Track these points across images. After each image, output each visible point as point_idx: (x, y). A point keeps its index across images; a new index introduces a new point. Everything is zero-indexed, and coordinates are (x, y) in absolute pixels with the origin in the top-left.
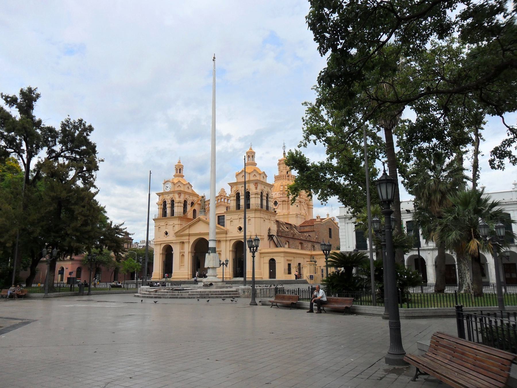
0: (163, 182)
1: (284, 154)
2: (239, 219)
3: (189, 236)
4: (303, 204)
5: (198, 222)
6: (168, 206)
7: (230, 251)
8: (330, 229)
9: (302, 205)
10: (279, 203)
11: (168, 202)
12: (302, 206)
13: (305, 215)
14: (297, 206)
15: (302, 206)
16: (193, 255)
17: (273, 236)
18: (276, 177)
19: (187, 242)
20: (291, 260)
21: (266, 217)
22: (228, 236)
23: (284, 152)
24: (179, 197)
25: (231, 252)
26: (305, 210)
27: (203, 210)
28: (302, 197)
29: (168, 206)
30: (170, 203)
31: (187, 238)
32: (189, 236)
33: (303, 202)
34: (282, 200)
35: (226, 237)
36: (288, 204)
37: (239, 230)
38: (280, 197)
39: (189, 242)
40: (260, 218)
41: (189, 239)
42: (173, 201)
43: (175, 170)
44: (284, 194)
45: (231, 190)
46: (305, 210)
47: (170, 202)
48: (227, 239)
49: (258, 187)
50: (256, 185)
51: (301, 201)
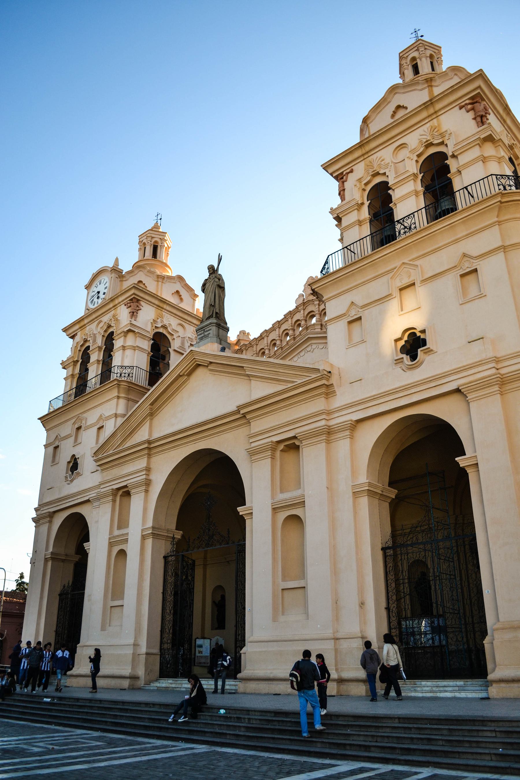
0: (86, 281)
2: (396, 293)
3: (149, 456)
6: (95, 356)
7: (356, 494)
16: (165, 548)
19: (137, 485)
22: (338, 401)
24: (133, 314)
25: (364, 501)
27: (213, 320)
29: (95, 356)
30: (100, 348)
31: (142, 463)
32: (149, 456)
35: (329, 413)
37: (404, 356)
39: (148, 483)
41: (148, 469)
42: (109, 339)
43: (140, 249)
47: (100, 341)
48: (336, 421)
50: (480, 107)
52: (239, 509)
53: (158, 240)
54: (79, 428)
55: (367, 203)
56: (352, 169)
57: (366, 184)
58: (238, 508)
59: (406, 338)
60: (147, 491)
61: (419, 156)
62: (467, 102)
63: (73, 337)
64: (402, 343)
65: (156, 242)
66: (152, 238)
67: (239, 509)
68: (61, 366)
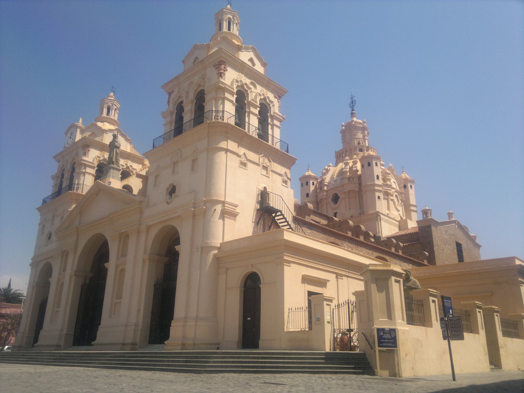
1: (352, 114)
4: (394, 198)
5: (97, 195)
6: (67, 175)
8: (459, 246)
9: (392, 200)
10: (341, 196)
11: (69, 167)
12: (391, 203)
13: (399, 219)
14: (379, 198)
15: (391, 203)
17: (276, 211)
18: (338, 154)
20: (322, 283)
21: (252, 156)
23: (353, 110)
26: (398, 211)
28: (388, 183)
29: (67, 175)
33: (392, 195)
34: (347, 190)
36: (359, 197)
38: (343, 186)
40: (223, 153)
41: (77, 241)
44: (351, 179)
45: (168, 102)
46: (398, 211)
49: (226, 73)
51: (389, 191)
52: (105, 264)
53: (111, 105)
54: (54, 216)
55: (175, 112)
56: (173, 91)
57: (176, 102)
58: (105, 264)
59: (171, 188)
60: (75, 252)
61: (196, 91)
62: (217, 63)
63: (59, 162)
64: (170, 190)
65: (109, 105)
66: (107, 103)
67: (105, 264)
68: (51, 178)
